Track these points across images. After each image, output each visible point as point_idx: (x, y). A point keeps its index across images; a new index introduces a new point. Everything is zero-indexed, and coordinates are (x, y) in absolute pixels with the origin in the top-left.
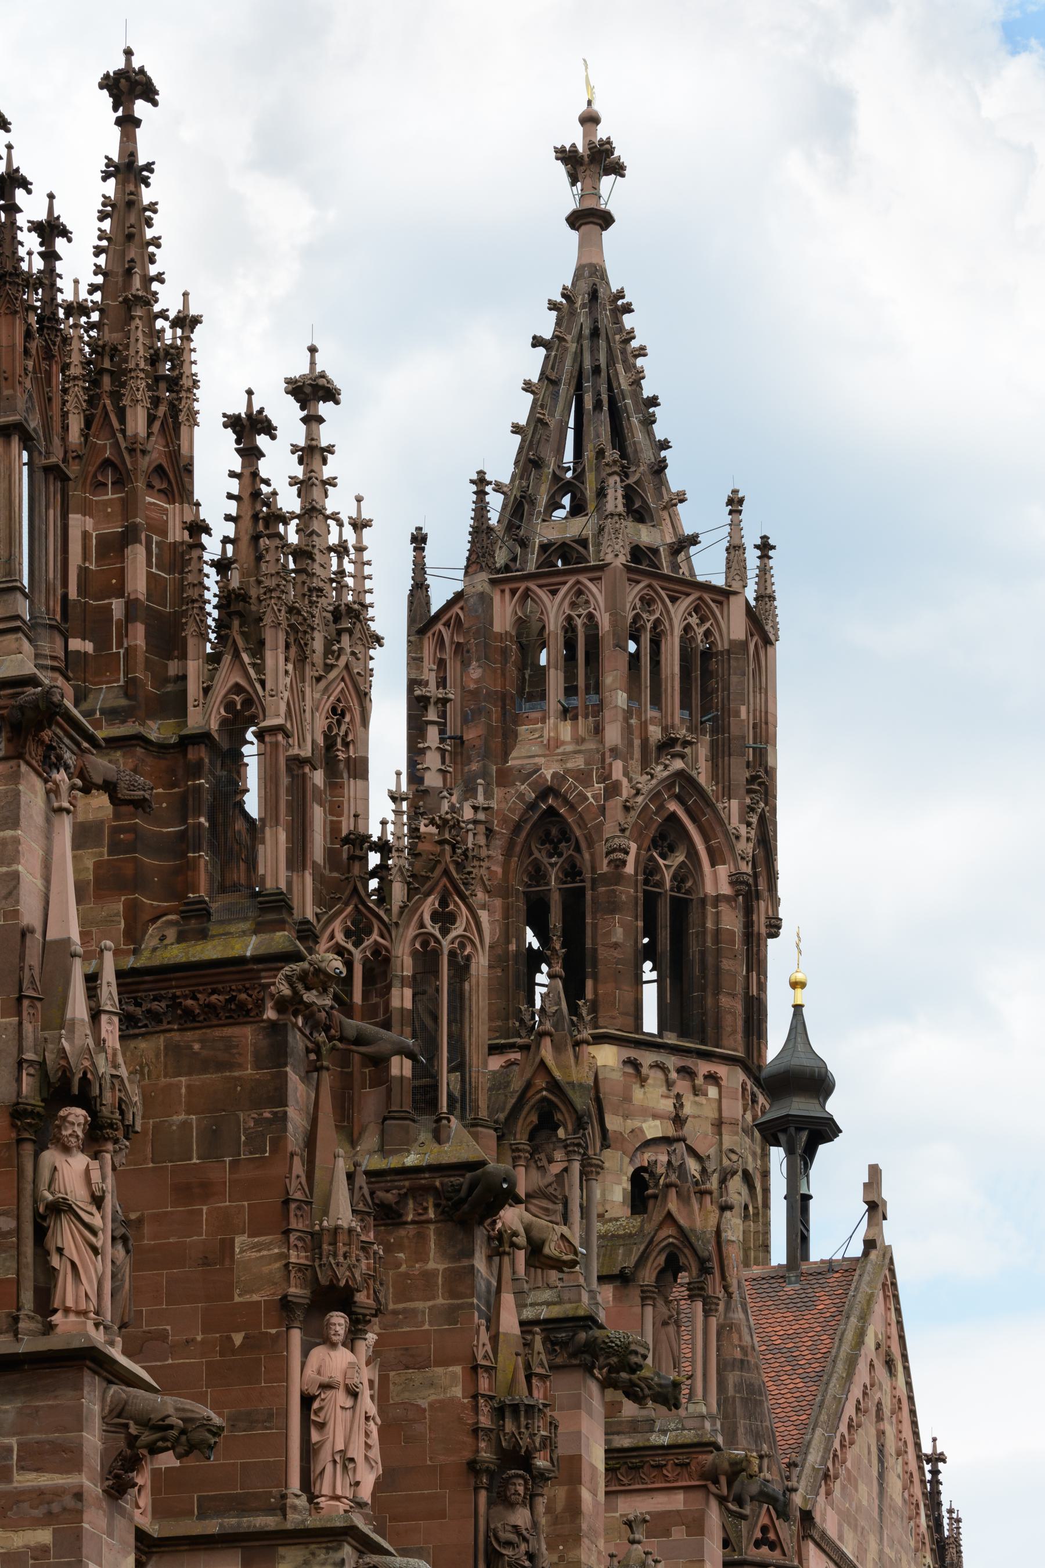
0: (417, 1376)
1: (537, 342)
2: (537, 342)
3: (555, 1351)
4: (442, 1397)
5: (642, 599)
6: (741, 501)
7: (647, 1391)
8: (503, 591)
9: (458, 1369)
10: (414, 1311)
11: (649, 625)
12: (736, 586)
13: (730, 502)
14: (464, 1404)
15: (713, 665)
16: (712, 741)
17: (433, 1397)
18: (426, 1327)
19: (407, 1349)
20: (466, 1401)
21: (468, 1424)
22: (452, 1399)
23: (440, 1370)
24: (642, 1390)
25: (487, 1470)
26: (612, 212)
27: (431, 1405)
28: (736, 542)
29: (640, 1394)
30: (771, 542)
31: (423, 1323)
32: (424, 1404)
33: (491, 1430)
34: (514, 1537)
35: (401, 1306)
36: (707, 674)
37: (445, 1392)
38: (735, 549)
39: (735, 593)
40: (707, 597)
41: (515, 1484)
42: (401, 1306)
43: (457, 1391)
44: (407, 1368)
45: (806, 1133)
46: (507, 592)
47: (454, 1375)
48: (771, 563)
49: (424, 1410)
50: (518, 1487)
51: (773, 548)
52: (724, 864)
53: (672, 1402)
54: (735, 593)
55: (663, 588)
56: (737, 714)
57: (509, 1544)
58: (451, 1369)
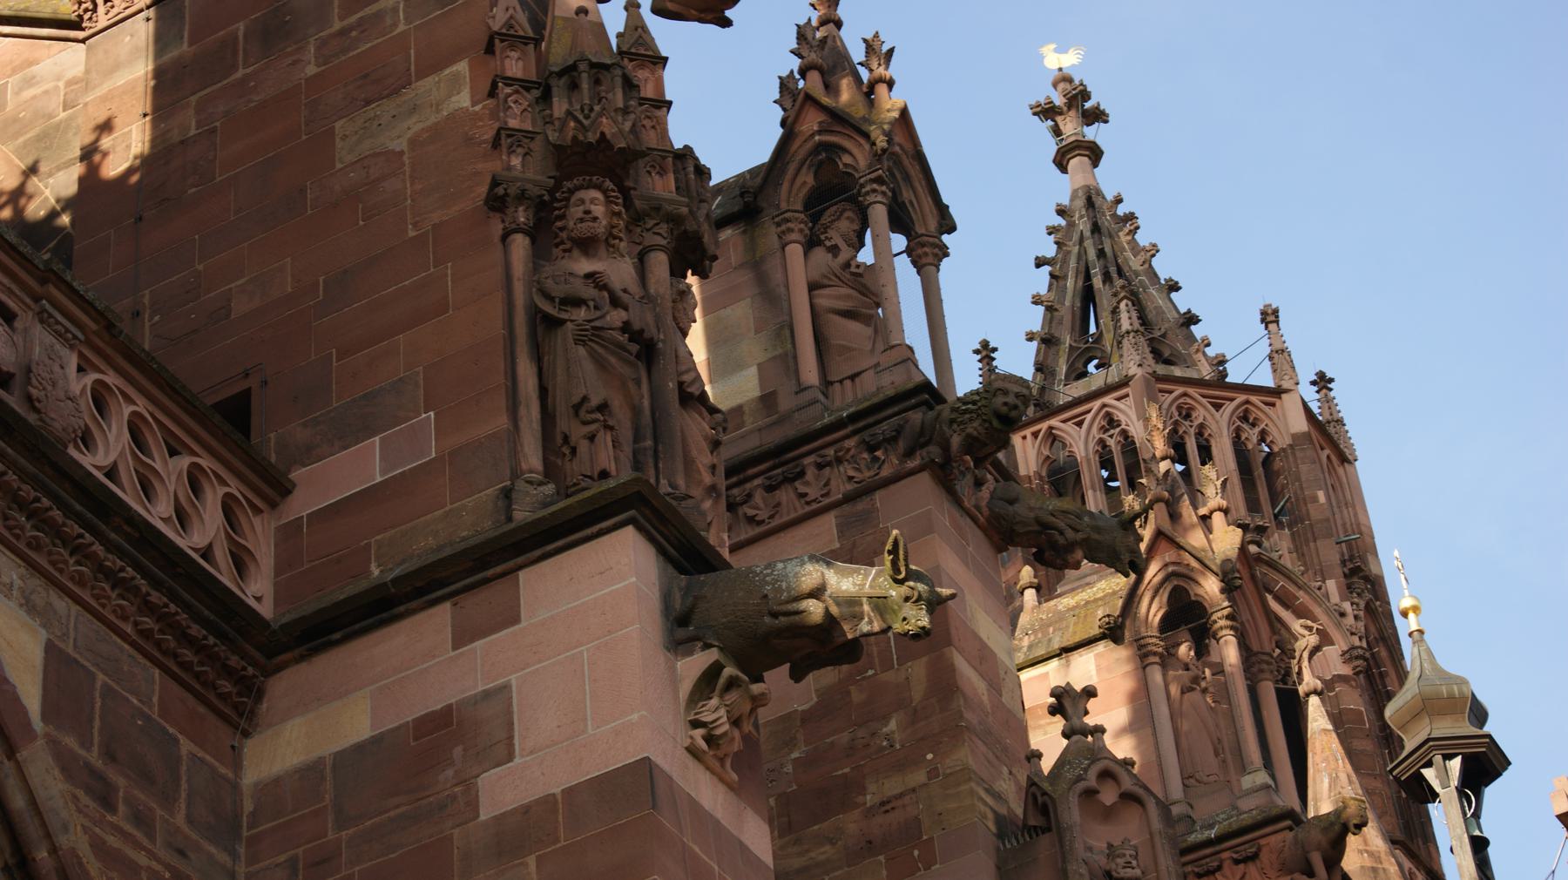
0: (388, 107)
1: (1040, 262)
2: (1040, 262)
3: (876, 459)
4: (433, 119)
5: (1179, 408)
6: (1276, 312)
7: (1070, 534)
8: (1024, 438)
9: (462, 67)
10: (379, 16)
11: (1192, 431)
12: (1286, 385)
13: (1264, 314)
14: (476, 113)
15: (1278, 464)
16: (1293, 534)
17: (417, 128)
18: (401, 27)
19: (366, 76)
20: (477, 108)
21: (485, 142)
22: (452, 117)
23: (428, 82)
24: (1061, 533)
25: (522, 197)
26: (1099, 142)
27: (413, 142)
28: (1278, 346)
29: (1061, 541)
30: (1329, 375)
31: (395, 25)
32: (400, 145)
33: (531, 136)
34: (589, 292)
35: (353, 19)
36: (1271, 476)
37: (438, 111)
38: (1279, 356)
39: (1287, 391)
40: (1254, 399)
41: (583, 201)
42: (353, 19)
43: (463, 100)
44: (368, 103)
45: (1458, 760)
46: (1029, 437)
47: (456, 77)
48: (1332, 394)
49: (402, 153)
50: (593, 207)
51: (1331, 380)
52: (1332, 644)
53: (1126, 558)
54: (1287, 391)
55: (1204, 396)
56: (1315, 499)
57: (578, 302)
58: (447, 71)
